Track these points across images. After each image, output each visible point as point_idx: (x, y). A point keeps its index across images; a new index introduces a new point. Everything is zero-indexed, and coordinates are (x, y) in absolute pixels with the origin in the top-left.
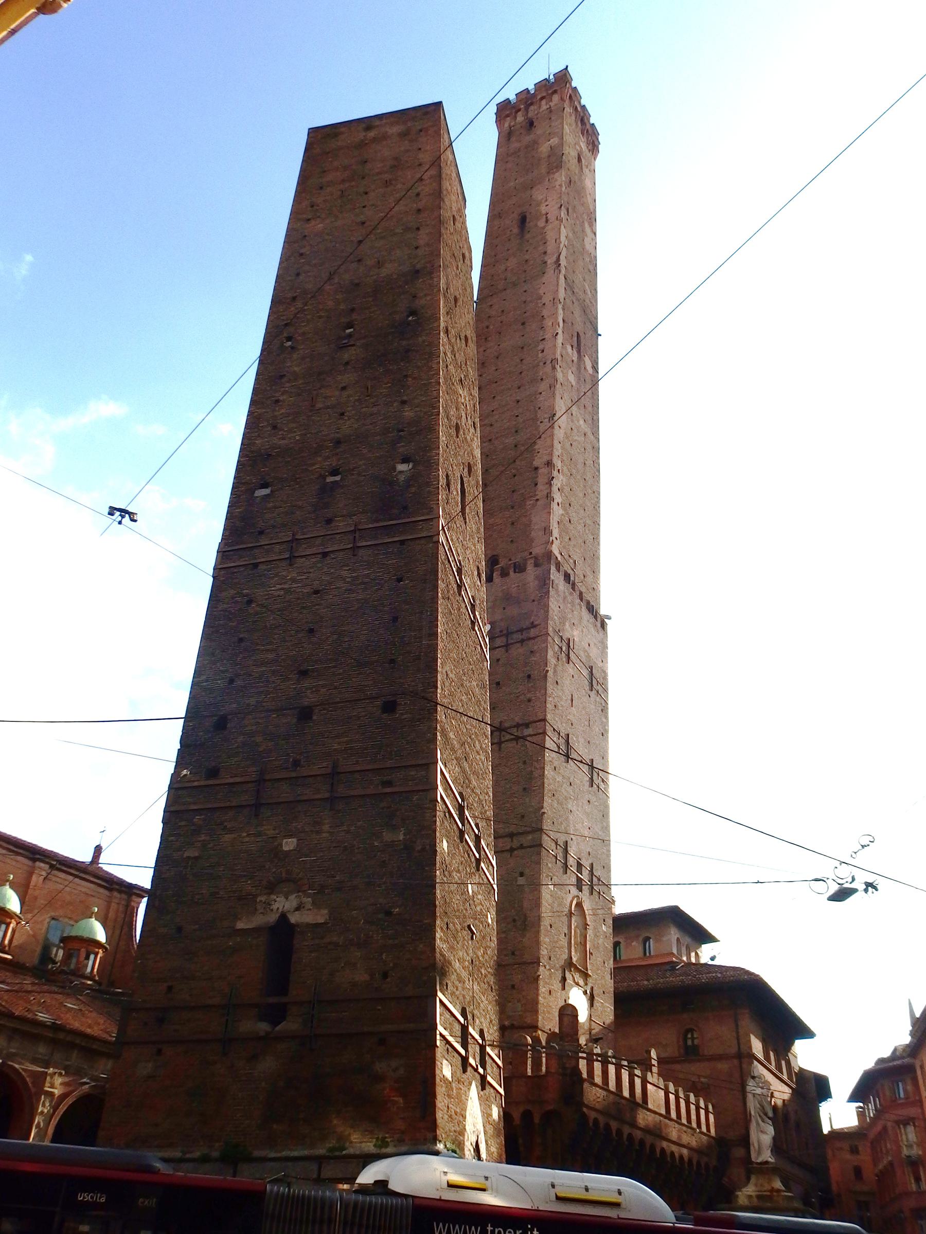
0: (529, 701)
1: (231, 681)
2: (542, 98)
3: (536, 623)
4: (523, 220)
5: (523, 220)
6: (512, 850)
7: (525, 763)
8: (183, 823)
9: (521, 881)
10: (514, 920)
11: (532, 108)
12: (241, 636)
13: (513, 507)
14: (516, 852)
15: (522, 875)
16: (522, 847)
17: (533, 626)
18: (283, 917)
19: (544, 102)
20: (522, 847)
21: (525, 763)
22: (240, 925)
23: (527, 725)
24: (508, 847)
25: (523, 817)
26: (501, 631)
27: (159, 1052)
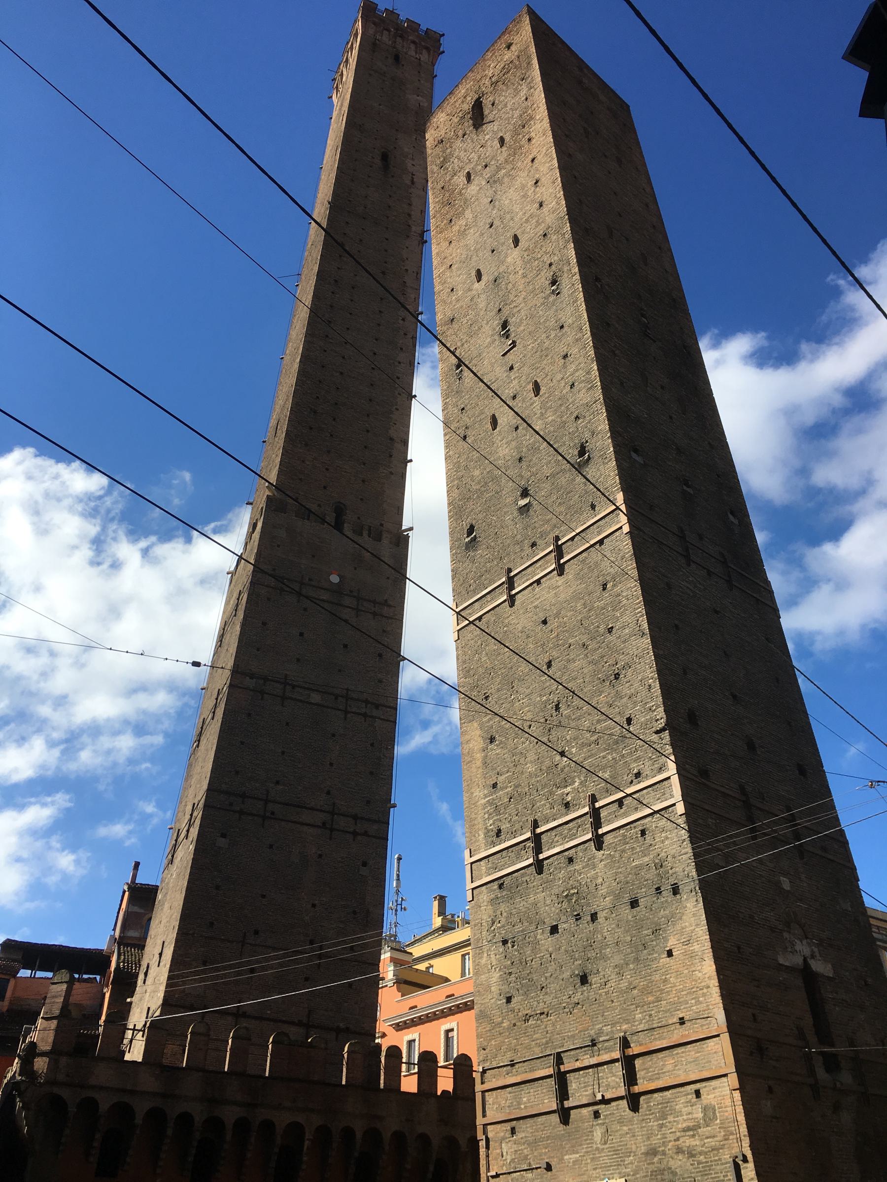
0: (380, 681)
1: (685, 673)
2: (414, 42)
3: (390, 603)
4: (385, 157)
5: (385, 157)
6: (355, 834)
7: (372, 745)
8: (700, 821)
9: (364, 871)
10: (355, 913)
11: (399, 40)
12: (676, 622)
13: (364, 464)
14: (359, 838)
15: (365, 864)
16: (366, 834)
17: (385, 603)
18: (805, 960)
19: (413, 46)
20: (366, 834)
21: (372, 745)
22: (781, 961)
23: (377, 706)
24: (351, 830)
25: (368, 802)
26: (351, 592)
27: (770, 1090)
